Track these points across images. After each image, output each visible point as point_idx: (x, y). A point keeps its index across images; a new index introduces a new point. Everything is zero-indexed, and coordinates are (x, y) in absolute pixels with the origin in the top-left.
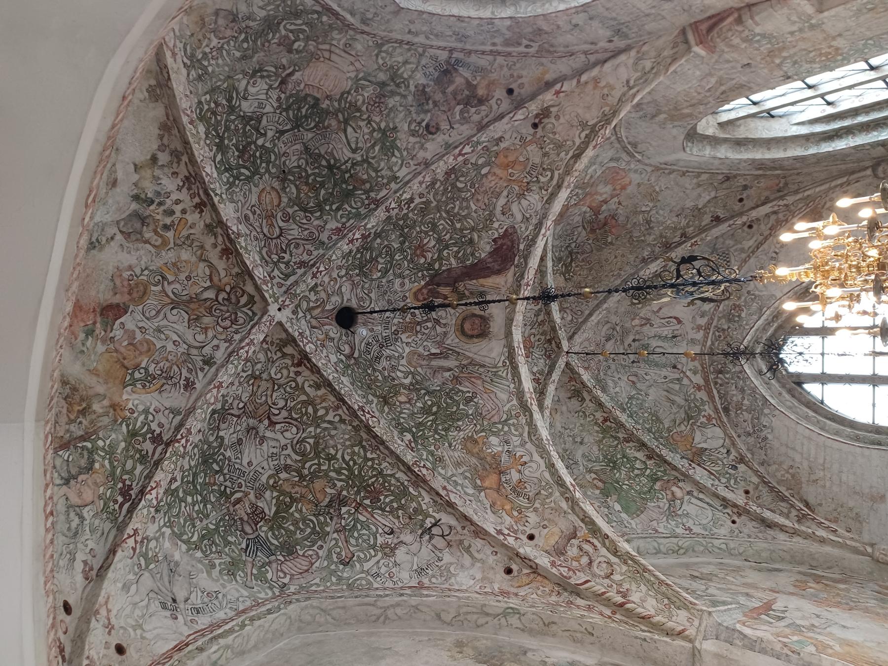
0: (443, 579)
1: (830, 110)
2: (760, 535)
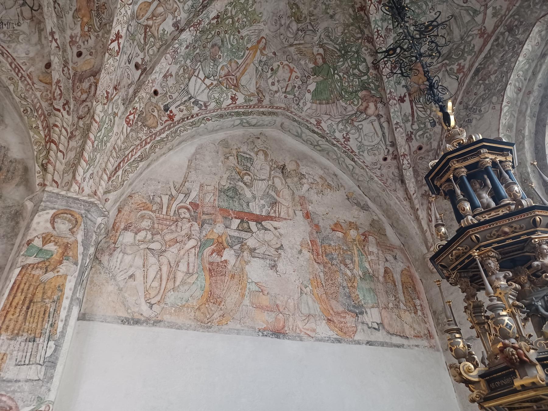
0: (9, 39)
2: (390, 181)
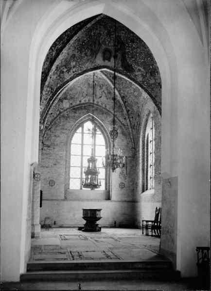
1: (149, 141)
